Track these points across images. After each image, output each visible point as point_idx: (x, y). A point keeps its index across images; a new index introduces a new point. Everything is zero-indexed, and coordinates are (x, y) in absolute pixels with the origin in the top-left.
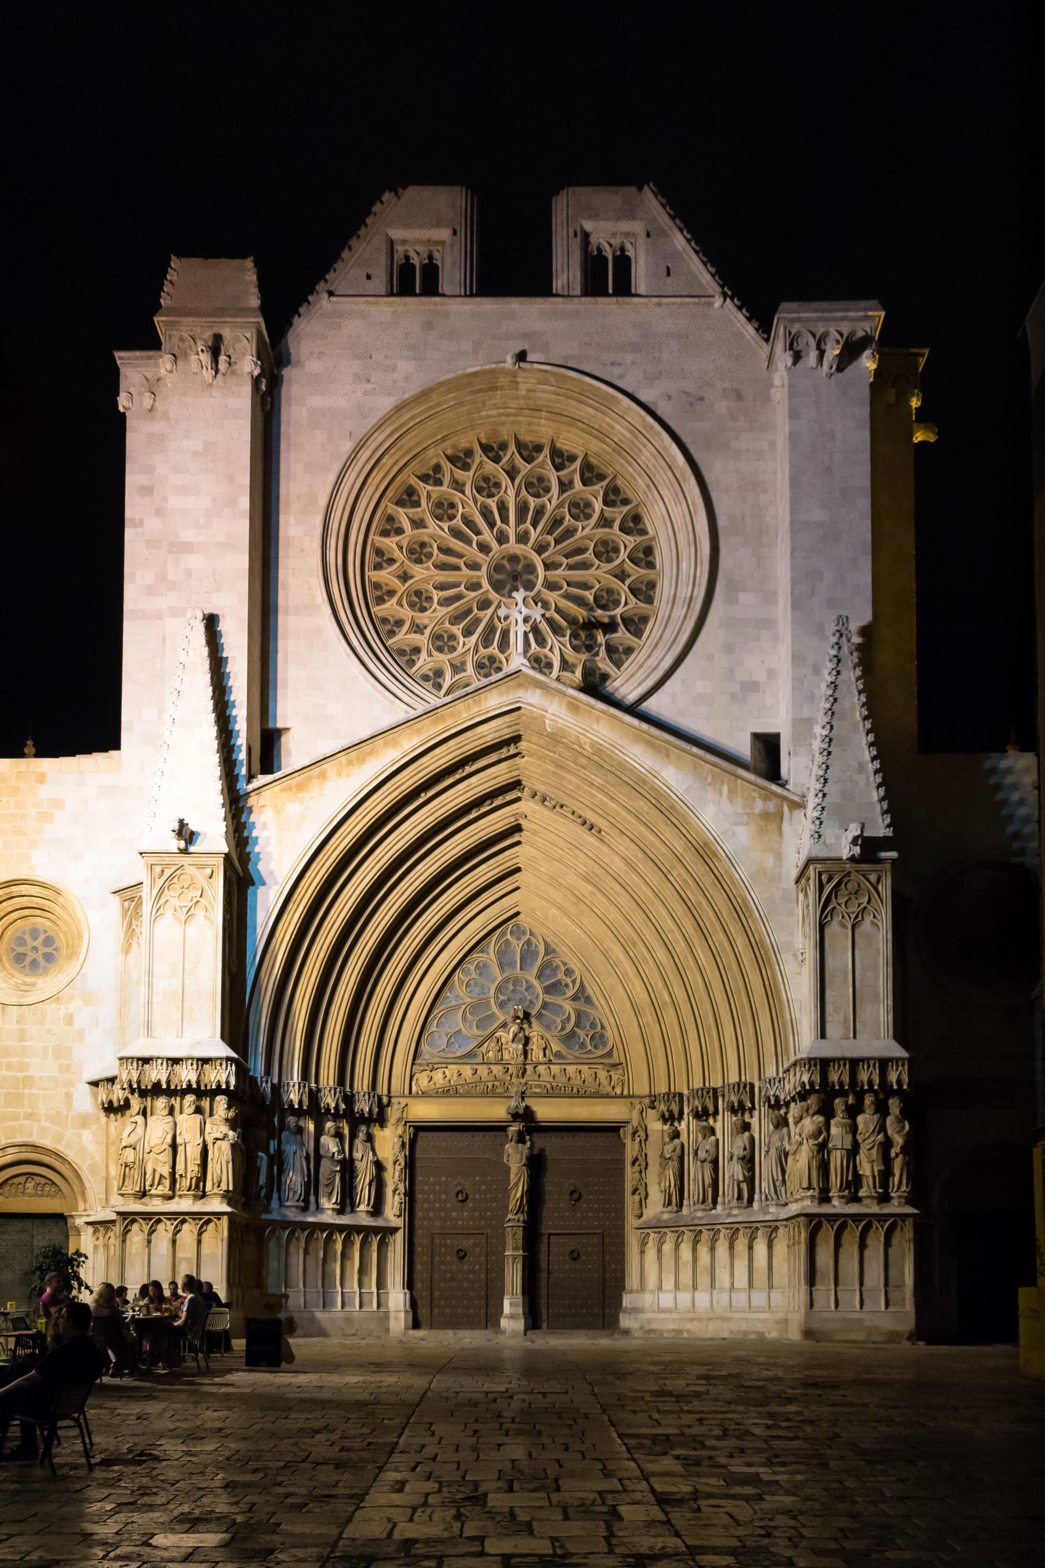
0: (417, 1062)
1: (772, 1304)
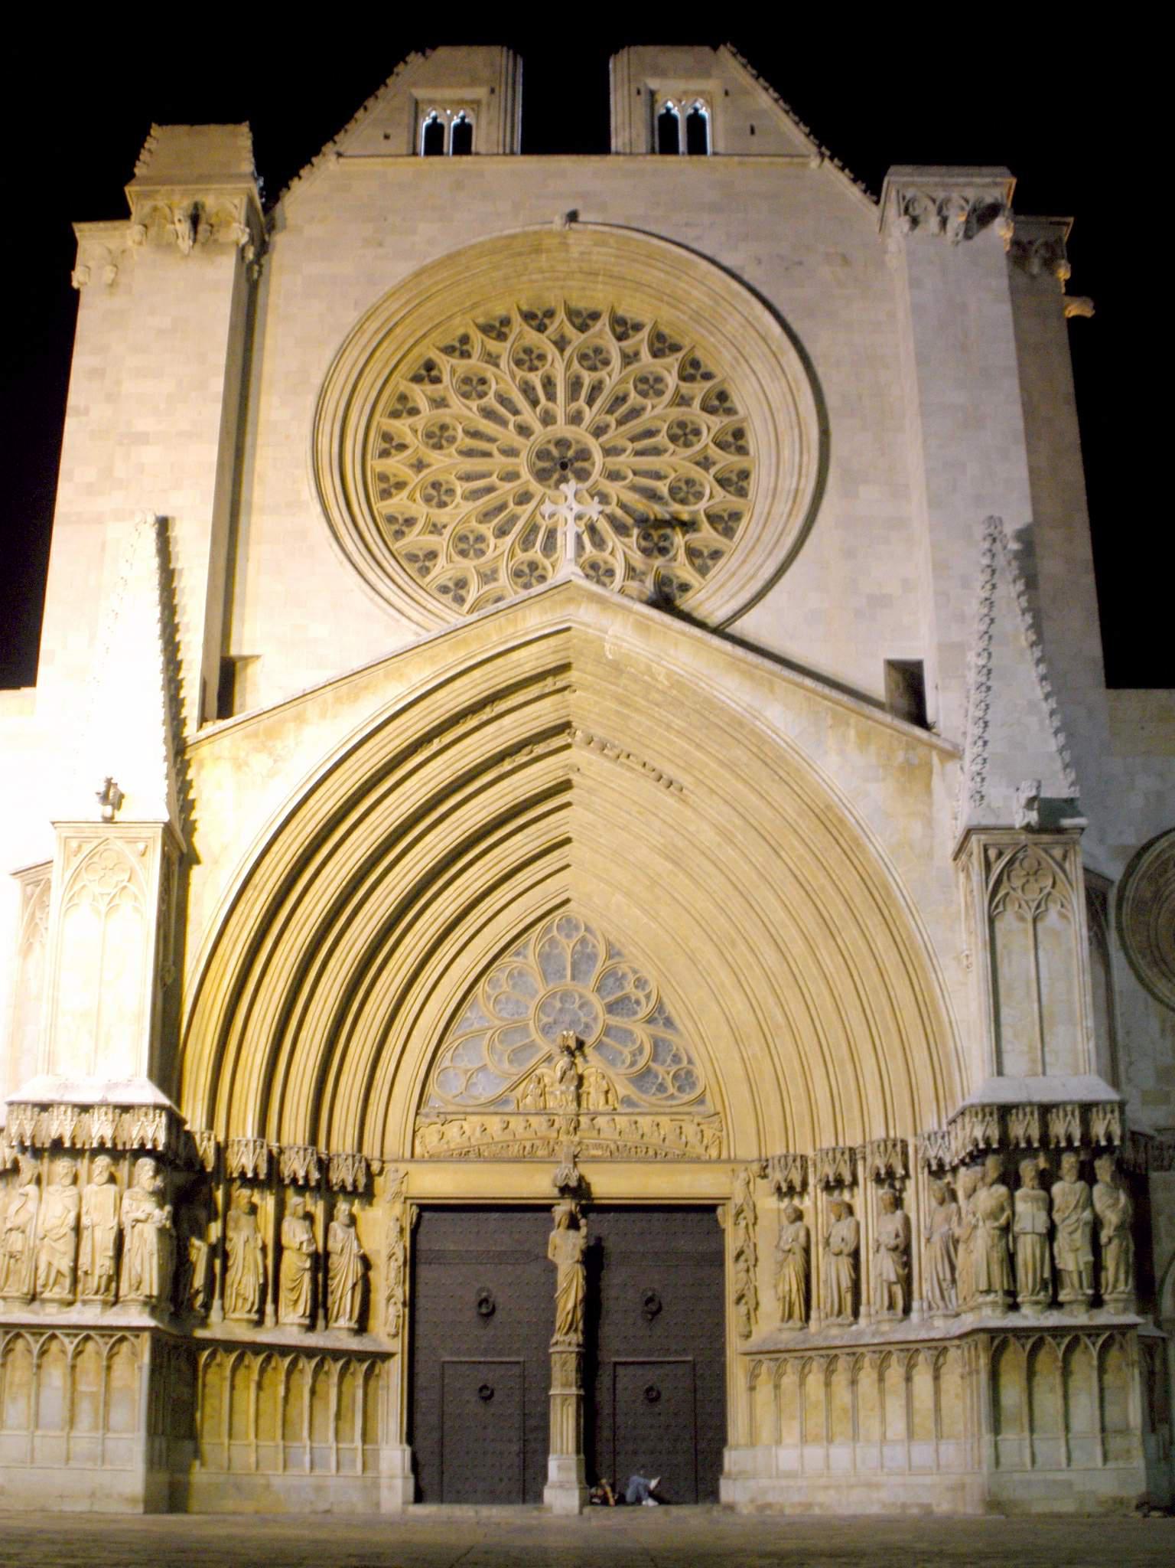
0: (423, 1110)
1: (943, 1462)
